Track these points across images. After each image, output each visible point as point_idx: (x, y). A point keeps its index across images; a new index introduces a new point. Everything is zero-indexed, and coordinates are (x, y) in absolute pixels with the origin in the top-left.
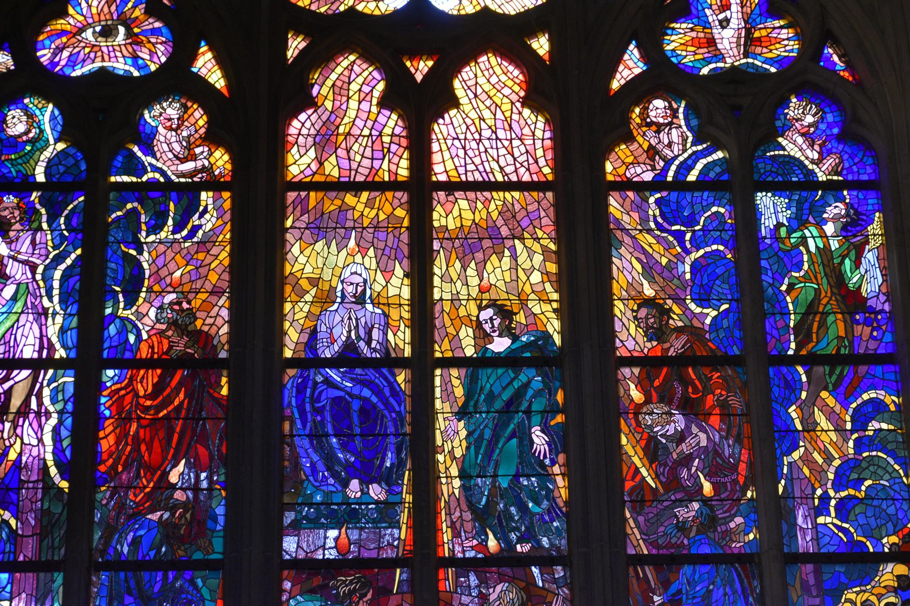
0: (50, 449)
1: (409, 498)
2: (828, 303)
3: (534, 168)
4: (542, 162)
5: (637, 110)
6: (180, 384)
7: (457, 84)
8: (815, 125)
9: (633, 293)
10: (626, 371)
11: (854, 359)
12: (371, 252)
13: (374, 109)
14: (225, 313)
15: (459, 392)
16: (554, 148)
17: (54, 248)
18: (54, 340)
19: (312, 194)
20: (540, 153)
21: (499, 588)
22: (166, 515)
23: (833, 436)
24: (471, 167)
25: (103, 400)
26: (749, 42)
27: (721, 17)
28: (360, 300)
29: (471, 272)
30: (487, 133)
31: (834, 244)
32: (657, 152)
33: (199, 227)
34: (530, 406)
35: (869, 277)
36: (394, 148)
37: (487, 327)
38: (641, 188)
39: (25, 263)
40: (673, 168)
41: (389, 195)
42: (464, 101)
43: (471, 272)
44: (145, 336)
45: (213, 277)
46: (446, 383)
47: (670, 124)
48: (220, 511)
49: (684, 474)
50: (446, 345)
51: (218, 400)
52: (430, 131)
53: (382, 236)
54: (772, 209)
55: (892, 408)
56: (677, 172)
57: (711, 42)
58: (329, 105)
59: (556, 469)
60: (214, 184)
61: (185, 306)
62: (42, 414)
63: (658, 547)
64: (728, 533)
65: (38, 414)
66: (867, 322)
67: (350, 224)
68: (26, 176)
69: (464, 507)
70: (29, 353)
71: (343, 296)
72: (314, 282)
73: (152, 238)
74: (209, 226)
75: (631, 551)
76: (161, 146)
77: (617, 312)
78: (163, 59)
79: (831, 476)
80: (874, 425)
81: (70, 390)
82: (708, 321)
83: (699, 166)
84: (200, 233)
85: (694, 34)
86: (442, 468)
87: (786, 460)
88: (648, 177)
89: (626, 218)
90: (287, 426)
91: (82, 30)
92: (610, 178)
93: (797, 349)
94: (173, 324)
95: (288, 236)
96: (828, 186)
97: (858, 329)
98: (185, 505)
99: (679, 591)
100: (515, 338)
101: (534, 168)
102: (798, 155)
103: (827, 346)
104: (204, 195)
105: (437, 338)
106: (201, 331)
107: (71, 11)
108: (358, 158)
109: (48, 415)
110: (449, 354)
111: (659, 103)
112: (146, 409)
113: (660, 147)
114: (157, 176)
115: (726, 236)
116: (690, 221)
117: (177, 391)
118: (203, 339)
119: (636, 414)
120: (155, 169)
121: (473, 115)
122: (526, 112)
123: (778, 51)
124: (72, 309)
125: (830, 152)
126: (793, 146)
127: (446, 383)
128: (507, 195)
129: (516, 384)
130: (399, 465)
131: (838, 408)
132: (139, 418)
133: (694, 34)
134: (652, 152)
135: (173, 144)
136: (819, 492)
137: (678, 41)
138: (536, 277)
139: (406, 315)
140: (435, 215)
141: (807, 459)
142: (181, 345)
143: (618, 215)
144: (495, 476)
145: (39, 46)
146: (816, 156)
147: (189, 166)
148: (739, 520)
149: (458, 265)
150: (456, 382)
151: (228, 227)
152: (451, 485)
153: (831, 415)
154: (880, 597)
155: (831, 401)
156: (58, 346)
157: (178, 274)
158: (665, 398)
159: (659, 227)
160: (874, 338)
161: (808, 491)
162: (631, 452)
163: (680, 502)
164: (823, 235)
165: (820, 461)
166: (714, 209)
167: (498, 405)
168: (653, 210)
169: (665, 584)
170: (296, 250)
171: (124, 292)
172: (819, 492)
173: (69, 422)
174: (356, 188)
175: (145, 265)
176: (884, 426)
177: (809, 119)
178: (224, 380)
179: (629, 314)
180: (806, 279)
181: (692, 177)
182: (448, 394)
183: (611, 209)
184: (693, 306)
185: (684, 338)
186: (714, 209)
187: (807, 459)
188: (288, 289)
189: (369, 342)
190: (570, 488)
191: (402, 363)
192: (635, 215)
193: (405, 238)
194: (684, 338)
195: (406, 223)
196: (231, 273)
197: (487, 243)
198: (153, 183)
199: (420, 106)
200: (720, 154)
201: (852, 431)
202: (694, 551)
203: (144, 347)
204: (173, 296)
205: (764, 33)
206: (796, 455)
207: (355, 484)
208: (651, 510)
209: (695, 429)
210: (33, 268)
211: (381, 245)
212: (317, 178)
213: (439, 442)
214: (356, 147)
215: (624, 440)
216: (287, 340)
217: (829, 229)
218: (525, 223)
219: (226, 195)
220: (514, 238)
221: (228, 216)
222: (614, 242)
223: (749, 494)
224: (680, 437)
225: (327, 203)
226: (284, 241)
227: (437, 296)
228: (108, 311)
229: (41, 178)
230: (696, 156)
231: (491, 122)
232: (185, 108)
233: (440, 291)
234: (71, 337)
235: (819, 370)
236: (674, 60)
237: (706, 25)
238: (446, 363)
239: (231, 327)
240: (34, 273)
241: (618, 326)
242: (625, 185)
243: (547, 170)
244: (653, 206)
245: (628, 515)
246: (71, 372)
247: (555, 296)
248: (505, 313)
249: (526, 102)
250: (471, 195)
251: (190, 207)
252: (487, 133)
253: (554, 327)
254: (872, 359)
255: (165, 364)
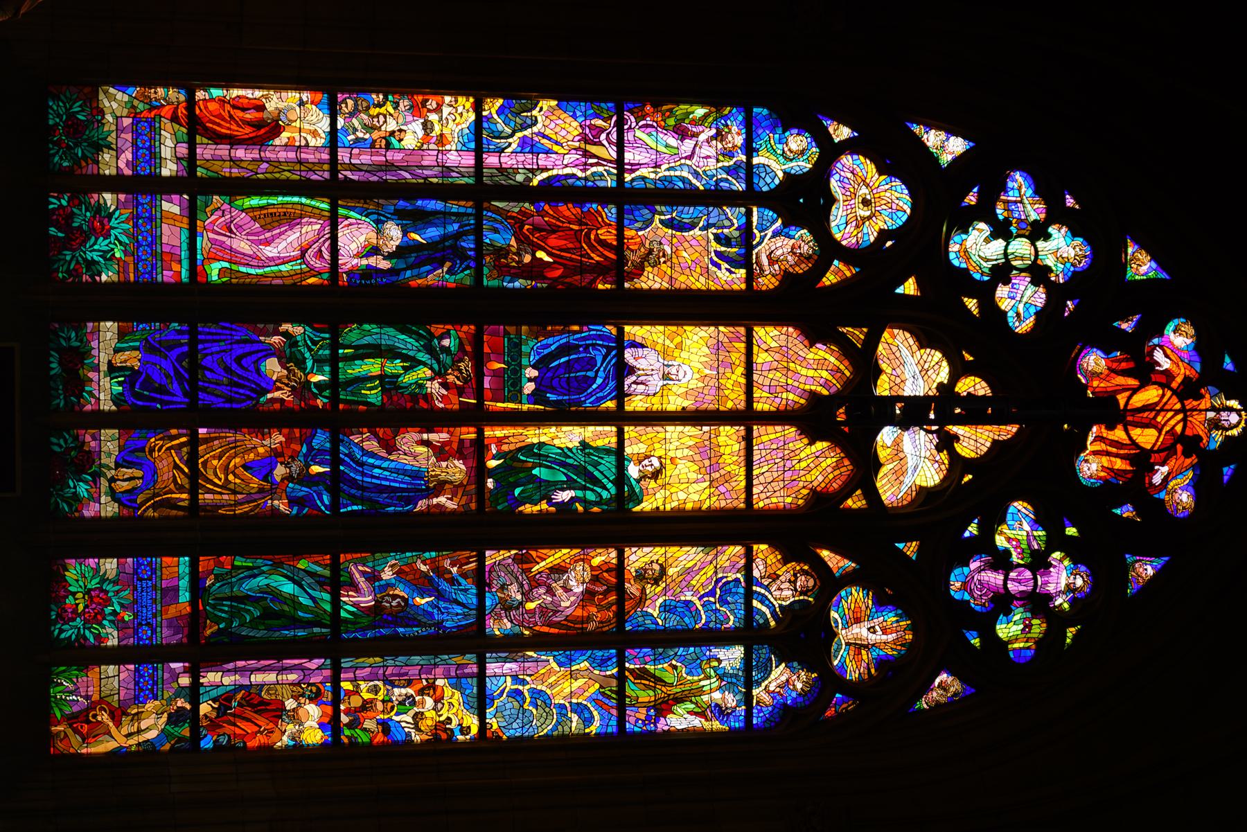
0: (560, 172)
1: (525, 407)
2: (661, 691)
3: (763, 496)
4: (767, 501)
5: (806, 567)
6: (606, 257)
7: (825, 444)
8: (795, 689)
9: (670, 561)
10: (614, 554)
11: (622, 708)
12: (700, 385)
13: (807, 387)
14: (657, 286)
15: (600, 443)
16: (777, 510)
17: (704, 171)
18: (637, 173)
19: (743, 345)
20: (774, 500)
21: (463, 467)
22: (514, 250)
23: (568, 691)
24: (764, 453)
25: (594, 206)
26: (858, 647)
27: (877, 628)
28: (666, 377)
29: (686, 452)
30: (788, 464)
31: (705, 698)
32: (774, 580)
33: (720, 268)
34: (589, 489)
35: (680, 720)
36: (778, 400)
37: (646, 462)
38: (748, 568)
39: (693, 152)
40: (763, 591)
41: (743, 397)
42: (813, 448)
43: (686, 452)
44: (640, 233)
45: (682, 278)
46: (606, 435)
47: (796, 590)
48: (517, 284)
49: (542, 591)
50: (633, 434)
51: (594, 281)
52: (791, 425)
53: (713, 392)
54: (732, 656)
55: (587, 731)
56: (759, 593)
57: (858, 621)
58: (811, 356)
59: (544, 506)
60: (750, 278)
61: (662, 260)
62: (585, 167)
63: (490, 572)
64: (500, 618)
65: (586, 164)
66: (648, 717)
67: (721, 370)
68: (757, 151)
69: (519, 445)
70: (628, 157)
71: (668, 366)
72: (679, 346)
73: (711, 237)
74: (719, 273)
75: (488, 553)
76: (779, 241)
77: (657, 549)
78: (844, 243)
79: (539, 688)
80: (575, 718)
81: (601, 184)
82: (650, 610)
83: (764, 609)
84: (715, 269)
85: (863, 608)
86: (546, 430)
87: (551, 659)
88: (756, 574)
89: (725, 558)
90: (576, 328)
91: (867, 186)
92: (755, 547)
93: (629, 670)
94: (651, 251)
95: (712, 328)
96: (748, 698)
97: (644, 711)
98: (520, 262)
99: (460, 584)
100: (638, 481)
101: (763, 496)
102: (772, 677)
103: (631, 689)
104: (743, 271)
105: (639, 428)
106: (643, 270)
107: (883, 177)
108: (771, 376)
109: (584, 170)
110: (626, 436)
111: (811, 583)
112: (588, 235)
113: (778, 582)
114: (757, 240)
115: (712, 625)
116: (723, 601)
117: (602, 255)
118: (639, 271)
119: (583, 560)
120: (762, 239)
121: (803, 455)
122: (805, 492)
123: (850, 666)
124: (659, 185)
125: (774, 698)
126: (779, 674)
127: (606, 435)
128: (742, 478)
129: (605, 481)
130: (546, 402)
131: (587, 694)
132: (581, 231)
133: (863, 608)
134: (775, 577)
135: (780, 246)
136: (528, 679)
137: (855, 597)
138: (682, 496)
139: (655, 408)
140: (728, 428)
141: (551, 672)
142: (631, 257)
143: (728, 552)
144: (540, 465)
145: (855, 157)
146: (772, 689)
147: (765, 261)
148: (509, 625)
149: (691, 443)
150: (606, 441)
151: (720, 288)
152: (533, 435)
153: (582, 690)
154: (456, 714)
155: (592, 690)
156: (633, 175)
157: (684, 254)
158: (595, 579)
159: (718, 581)
160: (638, 720)
161: (529, 672)
162: (557, 556)
163: (521, 585)
164: (711, 691)
165: (550, 681)
166: (732, 618)
167: (590, 468)
168: (731, 576)
169: (464, 575)
170: (702, 334)
171: (673, 219)
172: (528, 679)
173: (578, 183)
174: (749, 374)
175: (691, 233)
176: (574, 725)
177: (799, 686)
178: (608, 286)
179: (654, 558)
180: (680, 677)
181: (755, 603)
182: (598, 436)
183: (732, 548)
184: (661, 600)
185: (638, 594)
186: (732, 618)
187: (551, 672)
188: (674, 328)
189: (635, 383)
190: (532, 515)
191: (621, 405)
192: (727, 564)
193: (711, 407)
194: (638, 594)
195: (722, 408)
196: (686, 290)
197: (707, 463)
198: (753, 236)
199: (812, 418)
200: (773, 623)
201: (570, 703)
202: (487, 595)
203: (633, 233)
204: (668, 249)
205: (865, 657)
206: (554, 665)
207: (535, 373)
208: (516, 568)
209: (572, 599)
210: (690, 157)
211: (706, 392)
212: (755, 348)
213: (564, 428)
214: (779, 375)
215: (565, 551)
216: (637, 328)
217: (717, 696)
218: (722, 489)
219: (743, 286)
220: (711, 482)
221: (726, 287)
222: (708, 549)
223: (527, 633)
224: (567, 589)
225: (737, 355)
226: (709, 325)
227: (668, 428)
228: (658, 208)
229: (755, 161)
230: (771, 606)
231: (797, 467)
232: (809, 258)
233: (673, 431)
234: (639, 185)
235: (614, 683)
236: (843, 593)
237: (870, 618)
238: (620, 435)
239: (646, 290)
240: (686, 158)
241: (646, 550)
242: (749, 558)
243: (761, 504)
244: (734, 576)
245: (513, 552)
246: (614, 184)
247: (668, 507)
248: (656, 475)
249: (813, 491)
250: (742, 453)
251: (734, 263)
252: (788, 464)
253: (647, 506)
254: (622, 719)
255: (620, 246)
